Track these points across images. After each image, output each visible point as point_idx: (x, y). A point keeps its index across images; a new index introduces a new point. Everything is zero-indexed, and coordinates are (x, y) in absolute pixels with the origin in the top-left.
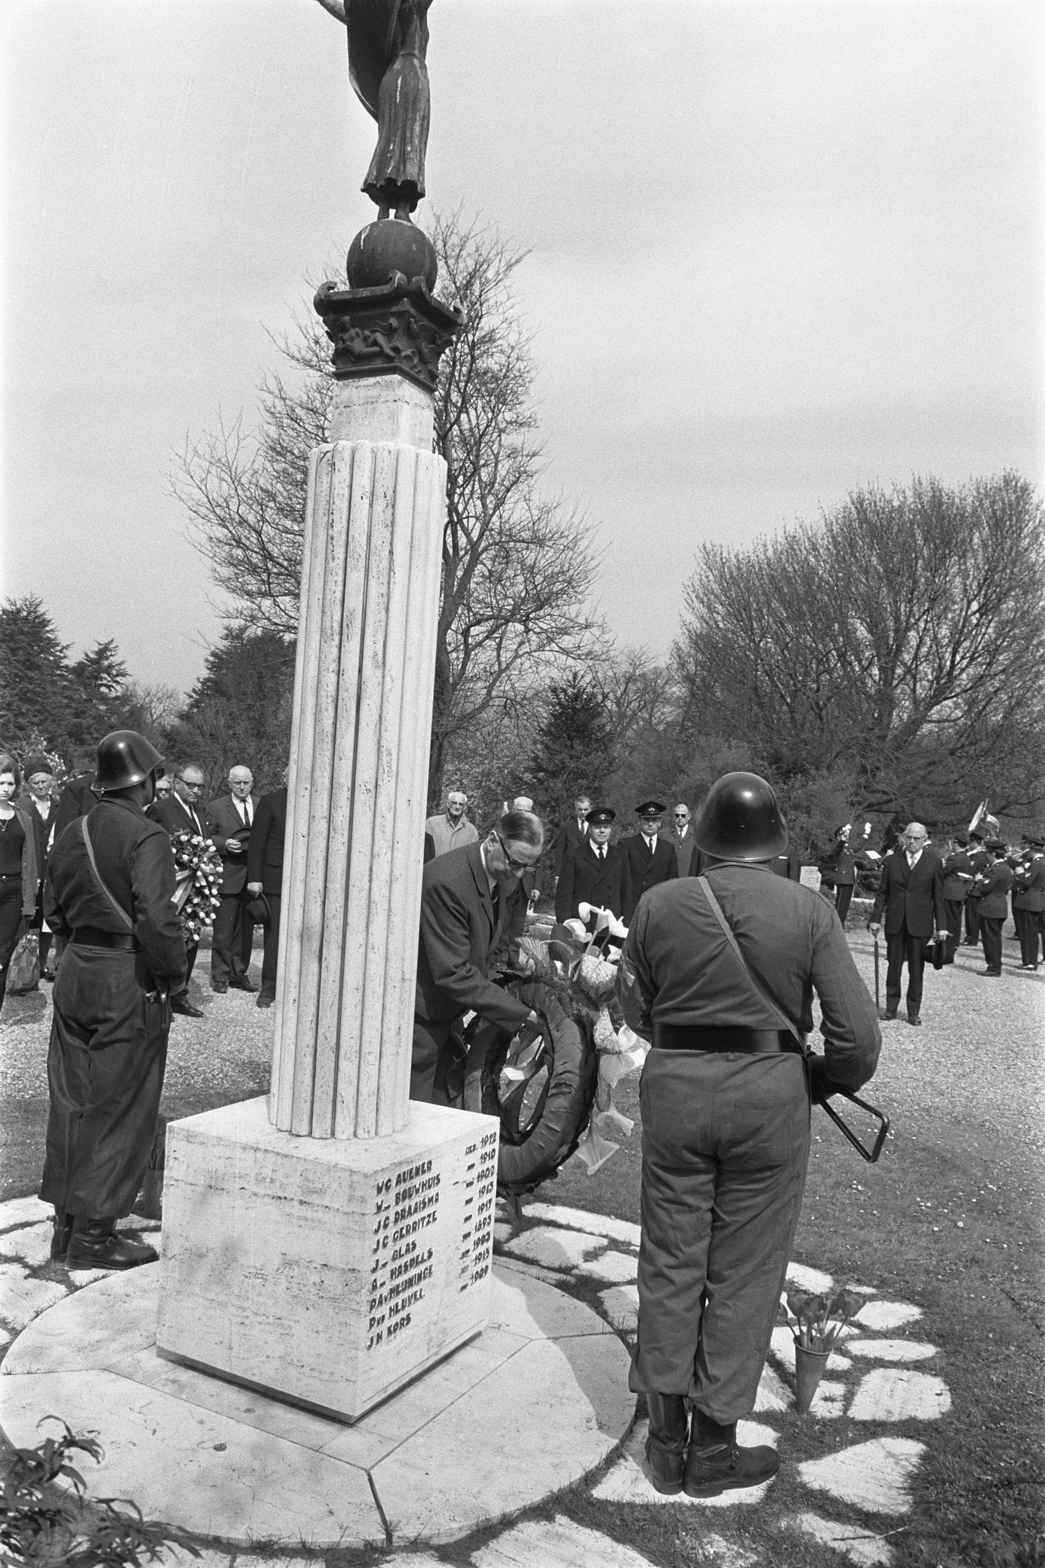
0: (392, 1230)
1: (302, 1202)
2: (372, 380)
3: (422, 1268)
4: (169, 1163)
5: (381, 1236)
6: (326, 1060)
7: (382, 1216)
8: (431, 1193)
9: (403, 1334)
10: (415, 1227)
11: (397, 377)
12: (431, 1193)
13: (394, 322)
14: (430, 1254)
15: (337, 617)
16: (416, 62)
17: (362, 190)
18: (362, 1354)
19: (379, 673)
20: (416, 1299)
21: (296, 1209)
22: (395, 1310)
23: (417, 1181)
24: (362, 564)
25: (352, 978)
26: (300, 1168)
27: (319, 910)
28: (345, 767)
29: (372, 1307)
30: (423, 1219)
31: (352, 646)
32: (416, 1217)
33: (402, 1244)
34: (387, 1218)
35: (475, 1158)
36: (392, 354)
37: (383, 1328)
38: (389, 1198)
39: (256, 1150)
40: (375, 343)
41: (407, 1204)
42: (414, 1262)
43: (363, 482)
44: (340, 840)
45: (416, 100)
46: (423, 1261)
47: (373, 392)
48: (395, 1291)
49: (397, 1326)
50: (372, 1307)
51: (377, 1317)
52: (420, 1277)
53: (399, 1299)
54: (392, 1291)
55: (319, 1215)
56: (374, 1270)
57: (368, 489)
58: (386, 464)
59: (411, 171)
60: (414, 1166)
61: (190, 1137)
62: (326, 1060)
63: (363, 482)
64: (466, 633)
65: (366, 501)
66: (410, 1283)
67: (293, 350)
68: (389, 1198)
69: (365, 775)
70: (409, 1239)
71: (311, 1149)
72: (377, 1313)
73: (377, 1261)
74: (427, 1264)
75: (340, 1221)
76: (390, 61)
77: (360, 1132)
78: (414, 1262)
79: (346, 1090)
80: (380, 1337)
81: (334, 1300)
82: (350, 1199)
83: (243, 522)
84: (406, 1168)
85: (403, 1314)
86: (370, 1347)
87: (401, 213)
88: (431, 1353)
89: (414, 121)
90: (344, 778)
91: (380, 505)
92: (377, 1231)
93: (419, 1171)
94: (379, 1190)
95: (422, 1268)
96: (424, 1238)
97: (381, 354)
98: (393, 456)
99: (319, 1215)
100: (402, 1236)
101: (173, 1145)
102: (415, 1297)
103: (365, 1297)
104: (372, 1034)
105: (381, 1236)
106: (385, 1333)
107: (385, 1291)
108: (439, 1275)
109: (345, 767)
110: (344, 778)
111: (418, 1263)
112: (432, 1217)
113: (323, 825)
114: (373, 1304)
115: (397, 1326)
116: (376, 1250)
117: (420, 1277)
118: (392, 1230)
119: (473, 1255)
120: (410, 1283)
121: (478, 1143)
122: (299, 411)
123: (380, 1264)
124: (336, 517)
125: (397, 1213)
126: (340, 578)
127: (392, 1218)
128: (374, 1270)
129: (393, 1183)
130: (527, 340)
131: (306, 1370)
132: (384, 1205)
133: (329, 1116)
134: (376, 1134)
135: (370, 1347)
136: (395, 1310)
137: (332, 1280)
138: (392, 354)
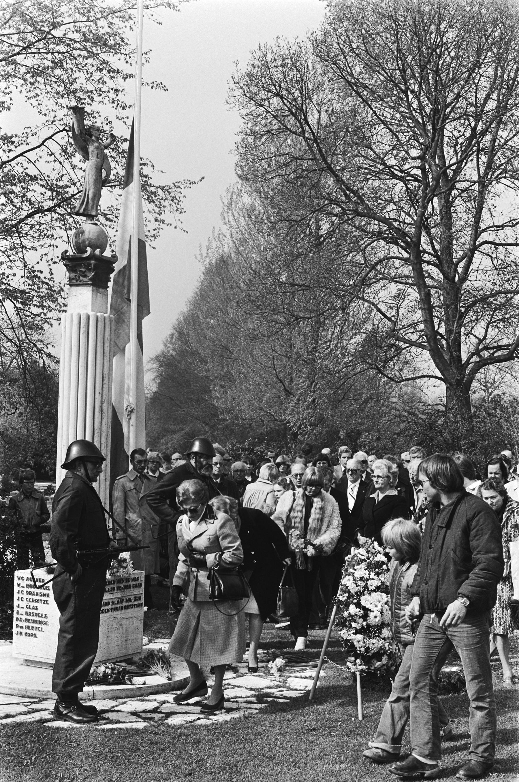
10: (37, 601)
22: (28, 627)
30: (41, 600)
32: (38, 598)
33: (32, 604)
48: (27, 620)
49: (30, 635)
52: (40, 623)
53: (31, 625)
54: (26, 620)
66: (35, 622)
70: (35, 604)
72: (20, 624)
85: (33, 632)
106: (24, 634)
107: (24, 617)
115: (30, 635)
117: (40, 623)
120: (35, 622)
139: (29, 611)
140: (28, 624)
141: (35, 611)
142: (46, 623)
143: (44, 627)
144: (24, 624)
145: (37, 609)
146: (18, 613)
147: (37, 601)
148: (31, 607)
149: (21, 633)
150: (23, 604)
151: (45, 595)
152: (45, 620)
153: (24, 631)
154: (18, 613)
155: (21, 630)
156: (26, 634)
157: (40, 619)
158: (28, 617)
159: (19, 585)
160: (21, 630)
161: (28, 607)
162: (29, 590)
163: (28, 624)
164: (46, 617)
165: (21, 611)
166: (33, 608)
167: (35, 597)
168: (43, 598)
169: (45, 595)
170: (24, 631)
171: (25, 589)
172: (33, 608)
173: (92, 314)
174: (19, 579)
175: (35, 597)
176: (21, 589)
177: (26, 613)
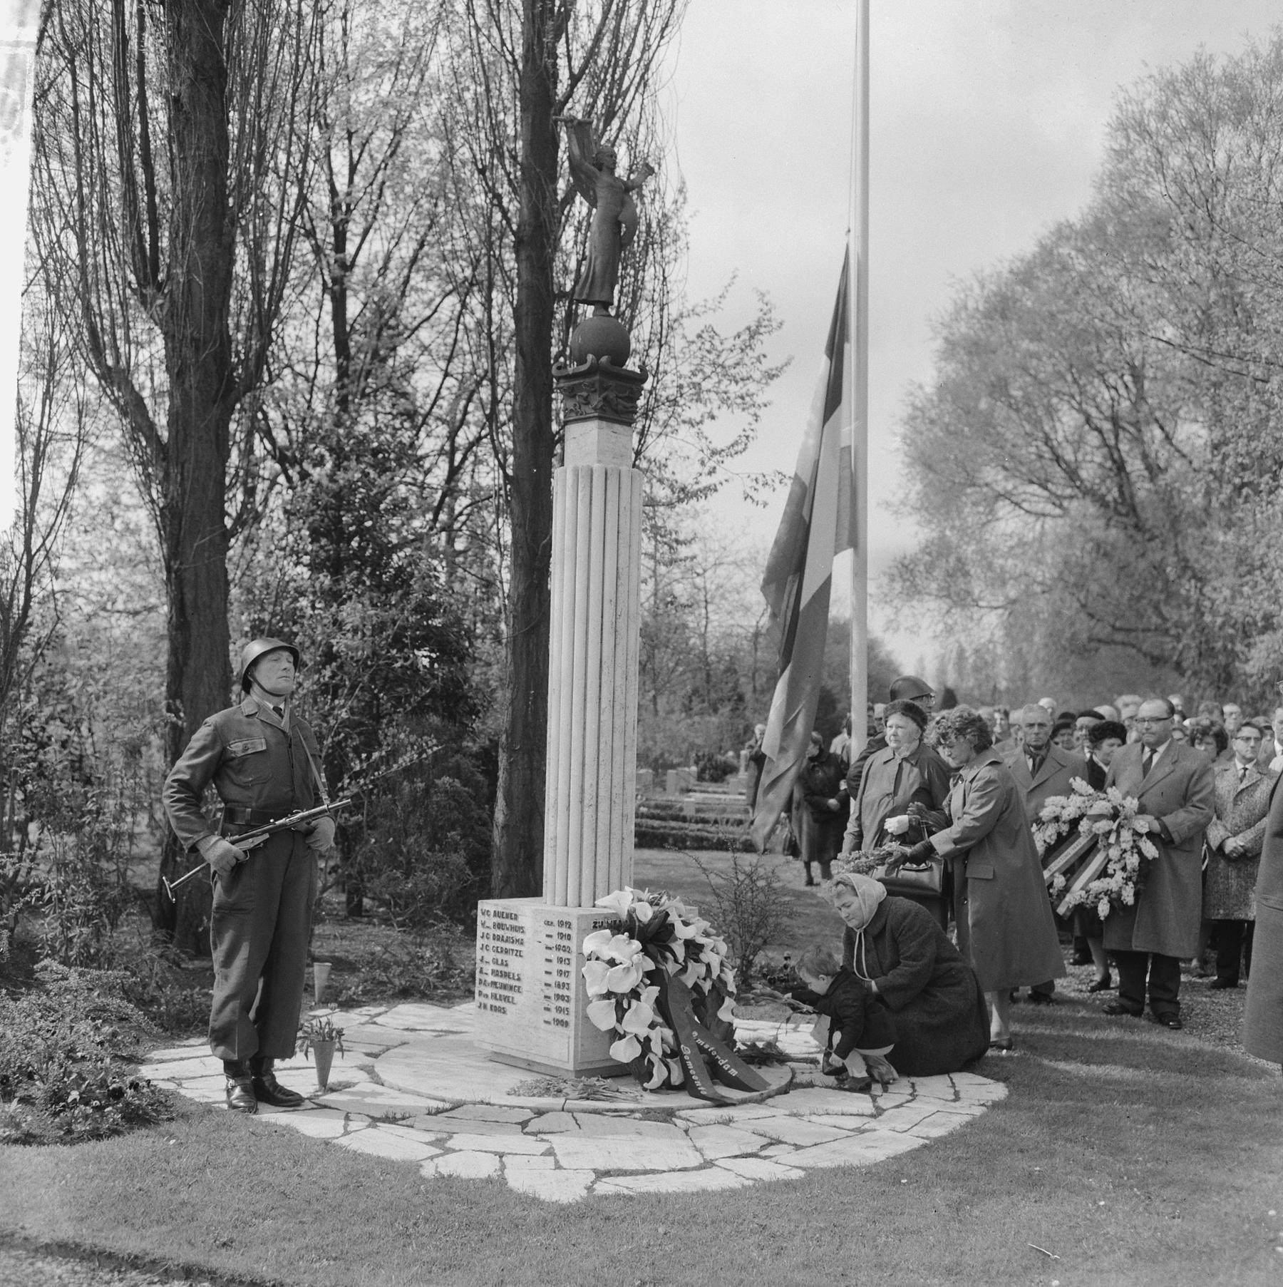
10: (507, 951)
22: (494, 996)
23: (508, 922)
33: (500, 957)
41: (500, 932)
42: (506, 975)
48: (494, 984)
52: (511, 988)
66: (504, 987)
78: (506, 975)
96: (515, 965)
107: (490, 978)
112: (519, 954)
117: (511, 988)
120: (504, 987)
136: (494, 996)
140: (495, 991)
143: (516, 996)
147: (507, 951)
149: (485, 1007)
150: (489, 956)
154: (481, 972)
159: (483, 924)
161: (496, 962)
164: (519, 979)
168: (516, 947)
170: (490, 1002)
173: (596, 466)
176: (486, 931)
177: (493, 971)
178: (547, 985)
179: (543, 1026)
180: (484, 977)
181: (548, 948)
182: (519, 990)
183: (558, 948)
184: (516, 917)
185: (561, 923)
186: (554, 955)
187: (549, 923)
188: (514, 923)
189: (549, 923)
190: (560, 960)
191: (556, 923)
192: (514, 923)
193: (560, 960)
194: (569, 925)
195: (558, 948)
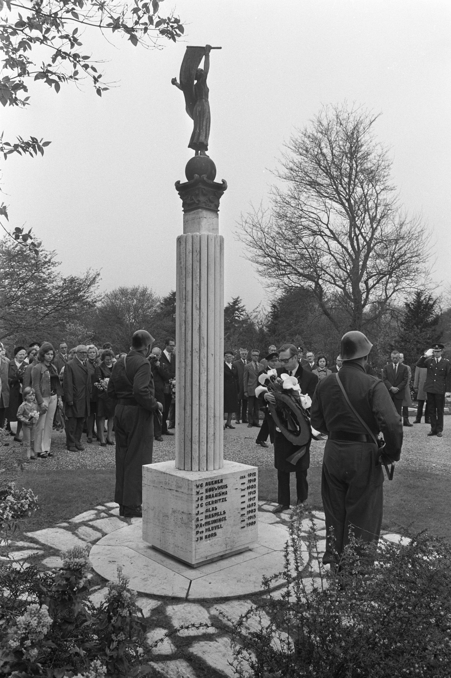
0: (204, 501)
1: (176, 491)
2: (193, 212)
3: (221, 517)
4: (143, 478)
5: (200, 502)
6: (188, 444)
7: (200, 496)
8: (224, 490)
9: (214, 539)
10: (216, 502)
11: (200, 210)
12: (224, 490)
13: (197, 192)
14: (224, 513)
15: (184, 293)
16: (204, 100)
17: (189, 146)
18: (194, 544)
19: (198, 312)
20: (218, 528)
21: (174, 493)
22: (208, 530)
23: (216, 486)
24: (191, 274)
25: (196, 415)
26: (176, 479)
27: (184, 393)
28: (189, 344)
29: (197, 527)
30: (220, 500)
31: (189, 303)
33: (210, 507)
34: (202, 497)
35: (245, 480)
36: (197, 202)
37: (204, 535)
38: (203, 490)
39: (164, 473)
40: (193, 200)
41: (211, 493)
42: (216, 514)
43: (189, 247)
44: (189, 368)
45: (204, 113)
46: (221, 514)
47: (194, 216)
49: (209, 536)
50: (197, 527)
51: (200, 531)
53: (210, 526)
54: (206, 523)
55: (181, 495)
56: (197, 514)
57: (191, 249)
58: (197, 240)
59: (202, 138)
60: (214, 480)
61: (148, 469)
62: (188, 444)
63: (189, 247)
64: (366, 283)
65: (191, 254)
66: (215, 521)
67: (282, 173)
68: (203, 490)
69: (196, 346)
70: (214, 506)
71: (182, 474)
73: (198, 512)
74: (224, 516)
75: (186, 497)
76: (196, 102)
77: (201, 469)
78: (217, 514)
79: (195, 455)
80: (201, 538)
81: (185, 524)
82: (188, 489)
83: (268, 246)
84: (210, 481)
85: (213, 532)
86: (197, 541)
87: (202, 153)
88: (228, 548)
89: (203, 120)
90: (189, 349)
91: (195, 254)
92: (197, 501)
93: (216, 482)
94: (198, 487)
95: (221, 517)
96: (221, 507)
97: (194, 203)
98: (198, 237)
99: (181, 495)
100: (210, 504)
101: (144, 473)
102: (217, 527)
103: (194, 523)
104: (203, 435)
105: (200, 502)
106: (204, 537)
107: (203, 522)
108: (229, 521)
109: (189, 344)
110: (189, 349)
111: (218, 515)
112: (225, 500)
113: (183, 364)
114: (197, 526)
115: (209, 536)
116: (197, 507)
117: (220, 520)
118: (204, 501)
119: (247, 516)
120: (215, 521)
121: (246, 475)
122: (287, 199)
123: (200, 512)
124: (182, 260)
125: (206, 496)
126: (184, 281)
127: (204, 497)
128: (197, 514)
129: (204, 485)
130: (386, 152)
131: (179, 548)
132: (200, 492)
133: (190, 463)
134: (207, 470)
135: (197, 541)
137: (185, 517)
138: (197, 202)
139: (208, 514)
140: (207, 527)
141: (214, 512)
142: (225, 519)
143: (222, 523)
144: (203, 529)
145: (216, 509)
146: (198, 520)
148: (211, 509)
151: (223, 493)
152: (224, 516)
153: (204, 535)
155: (201, 535)
156: (206, 536)
157: (219, 517)
158: (208, 520)
160: (201, 535)
162: (208, 494)
163: (207, 527)
165: (200, 517)
166: (213, 509)
167: (214, 499)
168: (221, 497)
169: (223, 493)
171: (204, 496)
172: (213, 509)
174: (198, 487)
175: (214, 499)
177: (206, 517)
178: (243, 509)
179: (240, 530)
180: (199, 523)
181: (243, 490)
182: (225, 519)
183: (248, 488)
184: (222, 481)
185: (250, 475)
186: (246, 493)
187: (242, 477)
188: (220, 485)
189: (242, 477)
190: (250, 493)
191: (246, 476)
192: (220, 485)
193: (250, 493)
194: (254, 474)
195: (248, 488)
